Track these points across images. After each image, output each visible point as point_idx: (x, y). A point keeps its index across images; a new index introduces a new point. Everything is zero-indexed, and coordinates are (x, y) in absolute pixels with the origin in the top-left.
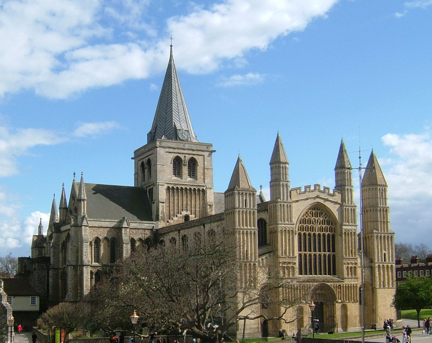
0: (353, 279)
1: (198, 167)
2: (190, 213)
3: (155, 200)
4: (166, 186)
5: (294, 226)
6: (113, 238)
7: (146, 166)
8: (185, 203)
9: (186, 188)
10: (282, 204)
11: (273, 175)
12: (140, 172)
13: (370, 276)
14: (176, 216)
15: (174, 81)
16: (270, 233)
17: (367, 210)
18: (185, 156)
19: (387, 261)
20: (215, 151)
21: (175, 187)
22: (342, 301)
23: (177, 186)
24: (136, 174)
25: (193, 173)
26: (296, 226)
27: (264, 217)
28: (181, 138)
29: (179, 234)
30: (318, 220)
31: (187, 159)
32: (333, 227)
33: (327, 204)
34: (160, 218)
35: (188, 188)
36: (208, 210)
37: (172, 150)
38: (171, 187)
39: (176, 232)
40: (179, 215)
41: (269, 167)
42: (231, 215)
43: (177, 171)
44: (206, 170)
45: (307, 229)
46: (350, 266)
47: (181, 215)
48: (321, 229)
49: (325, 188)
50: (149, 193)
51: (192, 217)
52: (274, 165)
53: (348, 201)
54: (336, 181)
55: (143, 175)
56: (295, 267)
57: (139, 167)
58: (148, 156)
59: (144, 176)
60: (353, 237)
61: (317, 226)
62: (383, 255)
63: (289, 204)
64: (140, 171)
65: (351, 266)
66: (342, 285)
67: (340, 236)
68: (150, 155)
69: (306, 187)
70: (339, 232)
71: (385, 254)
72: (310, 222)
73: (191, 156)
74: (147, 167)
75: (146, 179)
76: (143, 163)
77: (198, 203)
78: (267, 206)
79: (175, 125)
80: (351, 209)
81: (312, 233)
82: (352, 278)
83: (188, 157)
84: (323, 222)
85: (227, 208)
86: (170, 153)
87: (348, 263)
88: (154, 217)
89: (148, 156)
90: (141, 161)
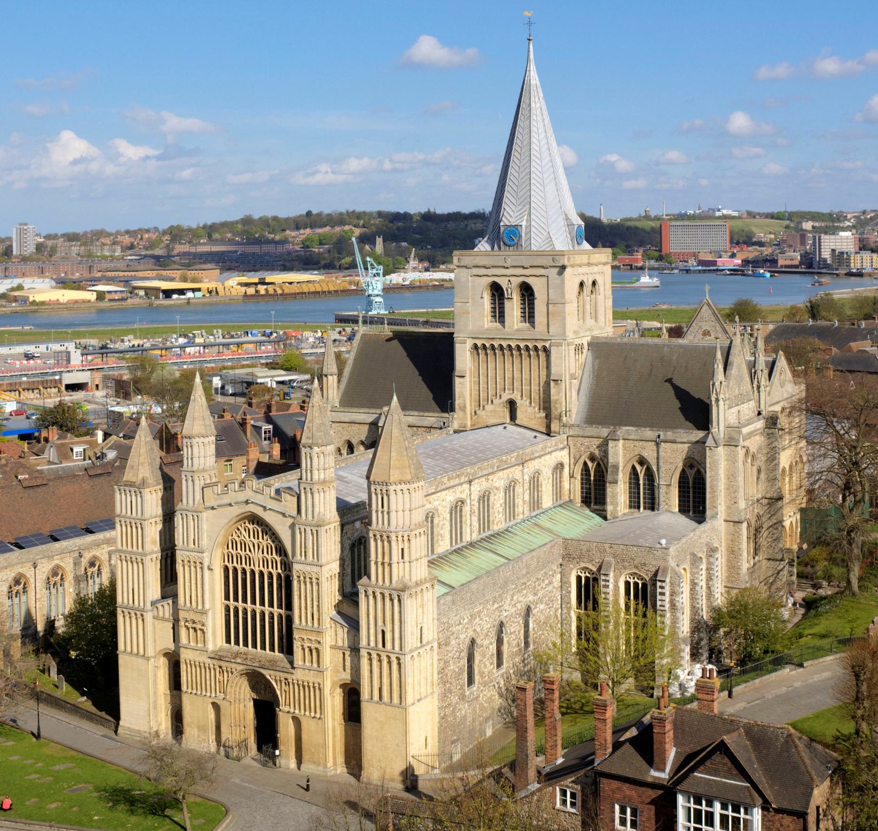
1: (536, 302)
2: (519, 397)
4: (469, 343)
8: (508, 375)
10: (184, 513)
21: (488, 345)
28: (507, 241)
34: (457, 407)
35: (513, 345)
40: (496, 401)
44: (550, 306)
46: (306, 645)
47: (501, 401)
48: (265, 562)
60: (315, 587)
71: (383, 632)
77: (534, 374)
81: (248, 569)
83: (516, 281)
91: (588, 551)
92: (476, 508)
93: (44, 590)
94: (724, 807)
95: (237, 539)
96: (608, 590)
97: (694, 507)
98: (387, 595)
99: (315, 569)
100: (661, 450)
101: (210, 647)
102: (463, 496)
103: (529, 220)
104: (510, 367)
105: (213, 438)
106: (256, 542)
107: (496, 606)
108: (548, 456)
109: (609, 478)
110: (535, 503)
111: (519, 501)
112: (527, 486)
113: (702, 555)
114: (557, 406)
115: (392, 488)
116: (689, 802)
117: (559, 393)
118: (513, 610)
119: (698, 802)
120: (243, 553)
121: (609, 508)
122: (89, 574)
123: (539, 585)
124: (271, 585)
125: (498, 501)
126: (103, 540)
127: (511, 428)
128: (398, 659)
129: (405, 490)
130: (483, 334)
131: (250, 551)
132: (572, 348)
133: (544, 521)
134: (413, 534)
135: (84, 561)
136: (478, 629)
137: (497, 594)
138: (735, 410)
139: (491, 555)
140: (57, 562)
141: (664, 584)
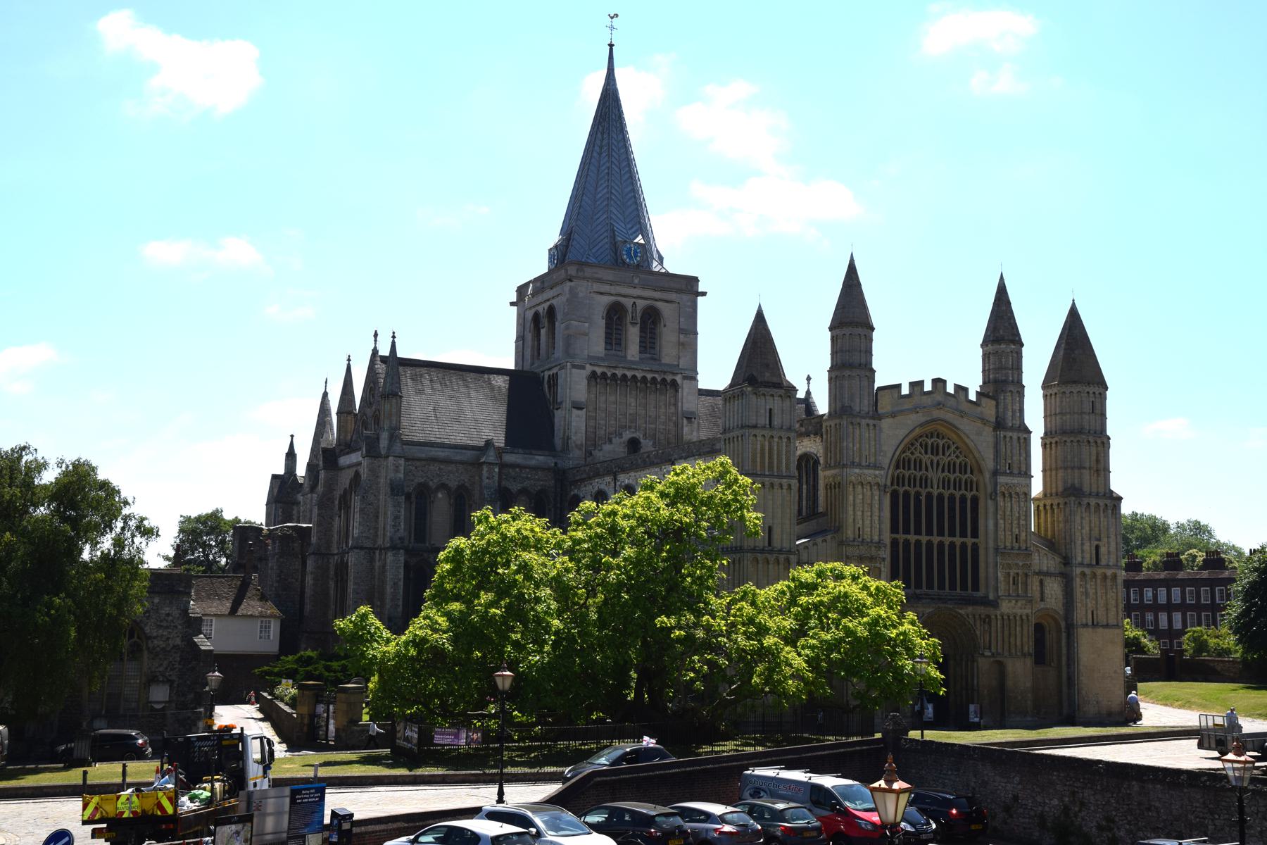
1: (664, 330)
2: (641, 436)
3: (561, 403)
4: (589, 368)
5: (886, 471)
6: (462, 487)
7: (545, 322)
11: (836, 352)
12: (529, 336)
13: (1061, 597)
14: (610, 441)
15: (614, 129)
16: (826, 488)
17: (1056, 442)
18: (634, 303)
19: (1103, 562)
20: (704, 294)
21: (609, 374)
22: (993, 654)
23: (614, 371)
24: (520, 338)
25: (649, 341)
26: (887, 472)
27: (812, 450)
29: (615, 483)
30: (938, 461)
31: (639, 308)
32: (975, 479)
33: (966, 426)
36: (686, 429)
37: (606, 288)
38: (599, 374)
39: (609, 479)
40: (616, 440)
41: (829, 334)
42: (736, 443)
45: (912, 481)
46: (1012, 572)
47: (622, 440)
48: (945, 484)
49: (957, 387)
50: (549, 387)
51: (647, 446)
52: (838, 332)
54: (984, 371)
55: (536, 343)
56: (883, 569)
57: (529, 325)
58: (548, 300)
59: (539, 344)
62: (1093, 548)
63: (871, 422)
64: (530, 334)
65: (1015, 571)
66: (993, 617)
67: (991, 499)
68: (553, 298)
69: (912, 385)
70: (989, 489)
71: (1097, 547)
72: (919, 465)
73: (648, 302)
74: (546, 324)
75: (543, 351)
76: (536, 317)
78: (821, 426)
79: (613, 231)
80: (1019, 438)
83: (641, 304)
85: (727, 426)
86: (602, 294)
87: (1009, 566)
88: (558, 442)
89: (548, 300)
90: (532, 311)
104: (633, 402)
124: (952, 509)
130: (598, 358)
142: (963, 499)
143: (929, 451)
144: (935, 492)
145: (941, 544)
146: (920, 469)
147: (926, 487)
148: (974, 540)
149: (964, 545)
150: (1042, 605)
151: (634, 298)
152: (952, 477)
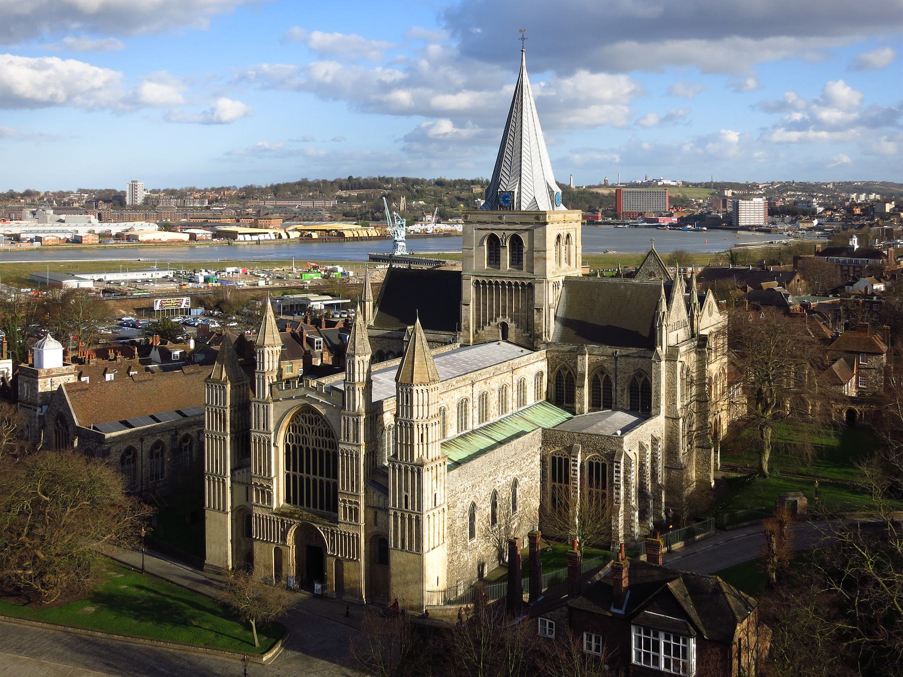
0: (352, 526)
9: (503, 282)
18: (504, 233)
34: (463, 327)
36: (536, 317)
37: (485, 226)
43: (494, 258)
47: (496, 323)
48: (317, 442)
53: (349, 406)
61: (311, 437)
71: (406, 497)
72: (301, 429)
73: (514, 232)
81: (304, 446)
82: (350, 524)
84: (321, 433)
86: (482, 229)
91: (562, 438)
92: (477, 404)
93: (148, 459)
94: (667, 638)
95: (296, 424)
96: (576, 468)
97: (642, 406)
98: (410, 468)
99: (355, 448)
100: (618, 362)
101: (275, 506)
102: (468, 395)
103: (520, 188)
104: (504, 300)
105: (280, 348)
106: (311, 427)
107: (492, 478)
108: (531, 366)
109: (578, 383)
110: (522, 401)
111: (509, 400)
112: (515, 388)
113: (648, 443)
114: (539, 328)
115: (415, 388)
116: (640, 633)
117: (540, 318)
118: (504, 482)
119: (647, 633)
120: (301, 435)
121: (578, 406)
122: (183, 447)
123: (524, 463)
125: (493, 400)
126: (194, 422)
127: (503, 343)
128: (417, 518)
129: (425, 391)
131: (306, 433)
132: (551, 285)
133: (529, 415)
134: (430, 423)
135: (179, 438)
136: (478, 496)
137: (492, 470)
138: (675, 333)
139: (488, 439)
140: (158, 438)
141: (619, 465)
142: (328, 452)
143: (307, 422)
144: (311, 448)
145: (315, 481)
146: (303, 433)
147: (306, 444)
148: (334, 480)
149: (328, 483)
150: (375, 529)
151: (503, 230)
152: (321, 438)
